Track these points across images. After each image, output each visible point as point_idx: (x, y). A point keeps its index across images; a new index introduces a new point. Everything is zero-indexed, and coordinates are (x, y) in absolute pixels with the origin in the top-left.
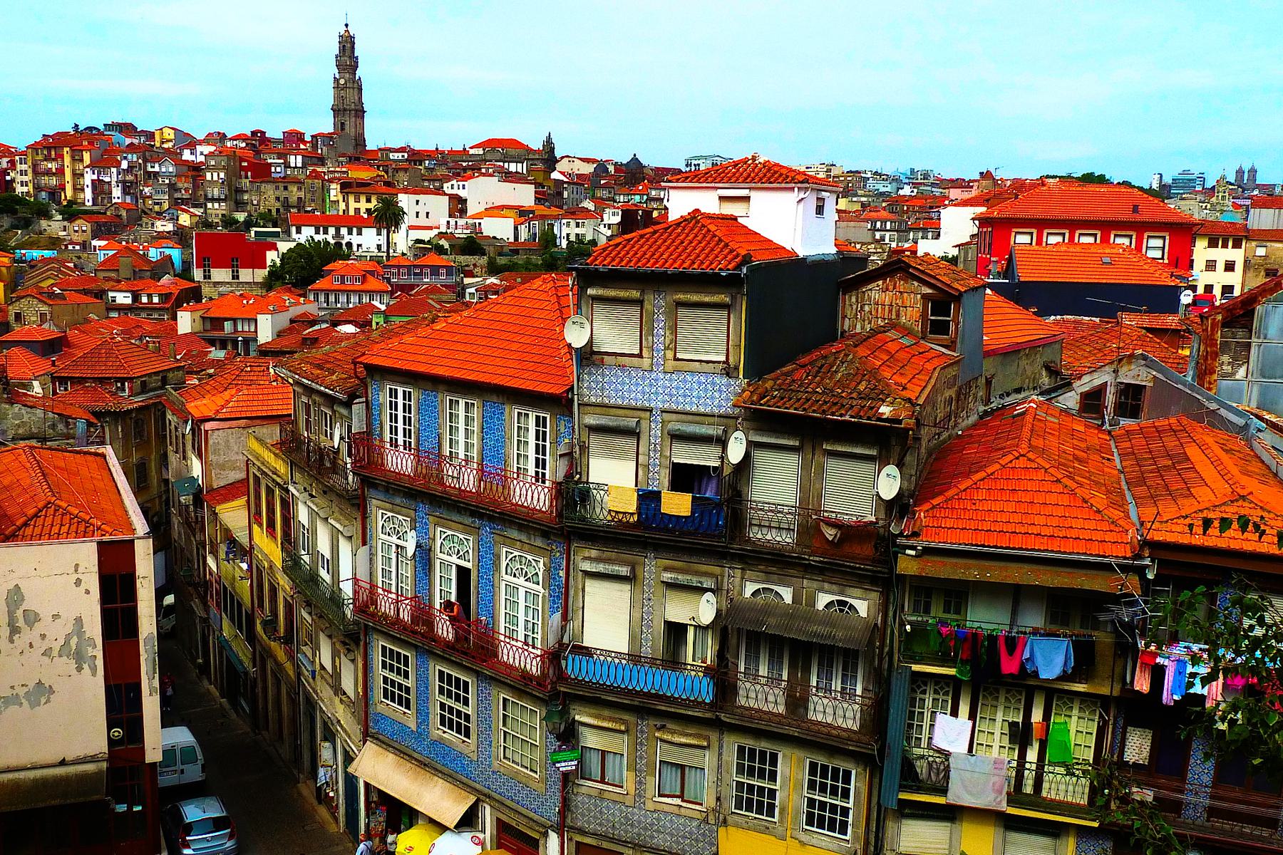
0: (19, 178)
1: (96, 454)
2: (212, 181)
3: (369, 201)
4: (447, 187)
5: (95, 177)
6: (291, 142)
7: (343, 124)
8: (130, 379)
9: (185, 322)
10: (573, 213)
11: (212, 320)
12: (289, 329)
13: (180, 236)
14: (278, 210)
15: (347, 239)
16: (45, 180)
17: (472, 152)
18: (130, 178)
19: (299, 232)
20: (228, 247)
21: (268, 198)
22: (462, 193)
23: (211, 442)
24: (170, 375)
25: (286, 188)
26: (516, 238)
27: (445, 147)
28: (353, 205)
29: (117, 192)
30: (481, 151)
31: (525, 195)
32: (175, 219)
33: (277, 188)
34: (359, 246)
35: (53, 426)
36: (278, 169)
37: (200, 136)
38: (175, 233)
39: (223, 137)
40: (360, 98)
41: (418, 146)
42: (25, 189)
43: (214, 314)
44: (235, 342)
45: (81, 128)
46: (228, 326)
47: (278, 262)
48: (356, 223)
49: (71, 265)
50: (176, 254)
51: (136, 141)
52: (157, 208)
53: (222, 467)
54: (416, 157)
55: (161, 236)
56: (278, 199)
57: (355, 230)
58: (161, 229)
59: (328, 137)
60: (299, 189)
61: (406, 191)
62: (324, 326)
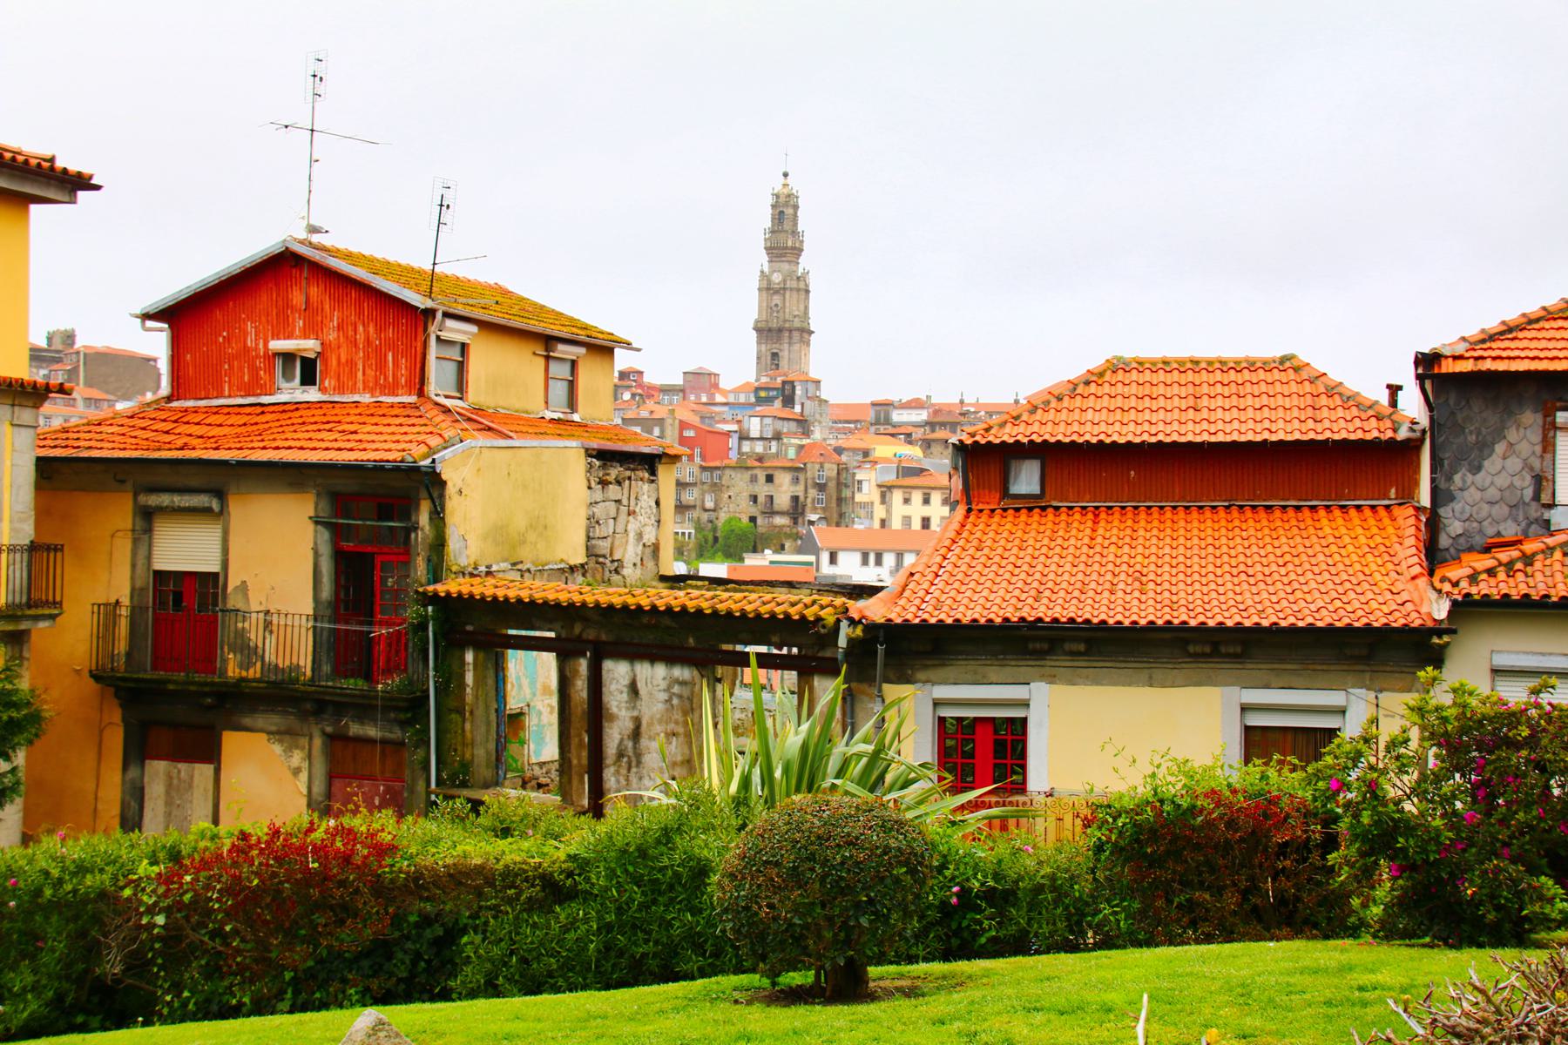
3: (926, 501)
6: (697, 389)
7: (775, 355)
25: (770, 479)
33: (754, 479)
40: (806, 308)
56: (755, 499)
60: (796, 481)
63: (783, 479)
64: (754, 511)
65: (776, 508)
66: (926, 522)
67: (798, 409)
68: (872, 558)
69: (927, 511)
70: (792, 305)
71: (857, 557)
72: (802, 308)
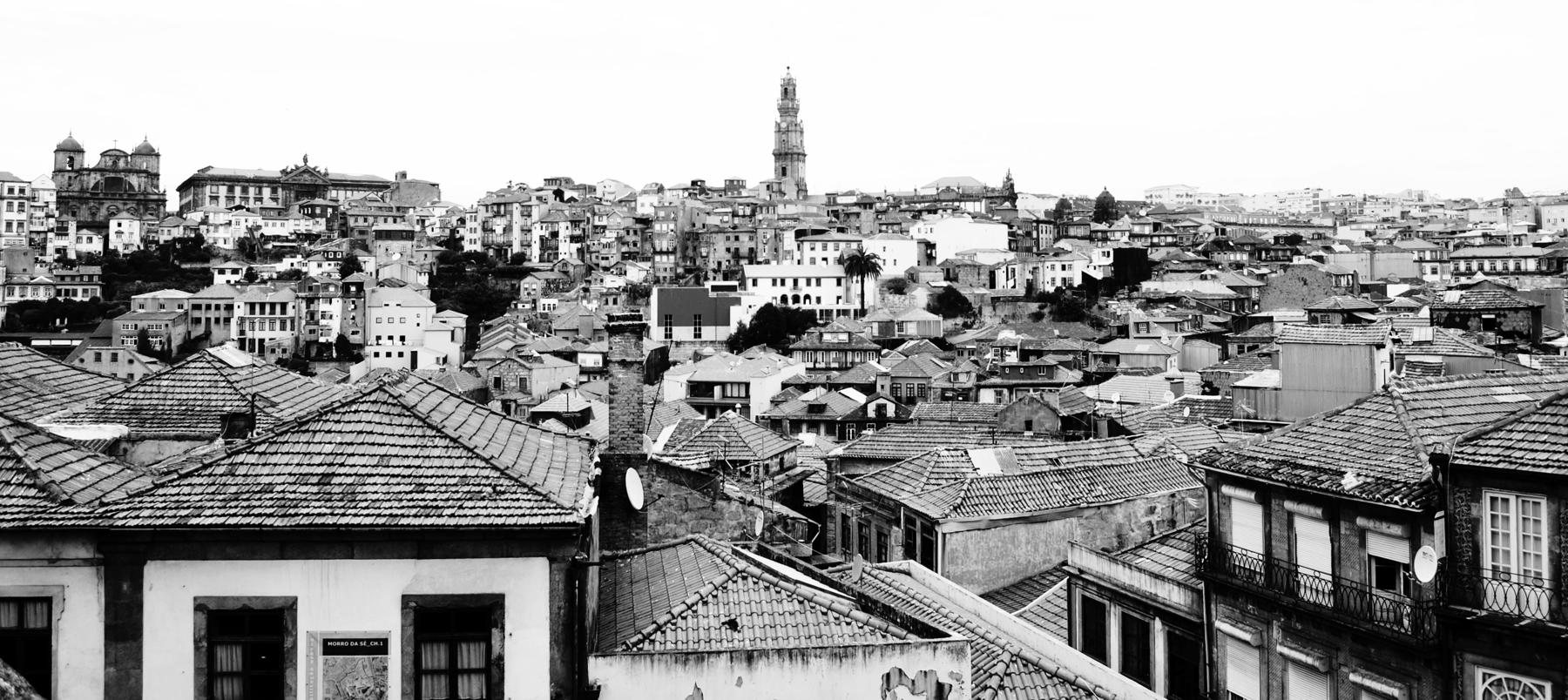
0: (468, 236)
2: (661, 235)
3: (825, 248)
4: (913, 230)
7: (784, 170)
10: (1056, 255)
13: (637, 294)
18: (578, 232)
19: (755, 283)
20: (694, 304)
22: (931, 239)
23: (948, 548)
24: (786, 456)
25: (737, 238)
30: (934, 192)
33: (728, 239)
36: (726, 218)
37: (638, 189)
39: (661, 189)
41: (867, 191)
46: (717, 389)
47: (747, 322)
51: (575, 194)
52: (603, 263)
54: (866, 203)
56: (728, 250)
57: (813, 282)
60: (751, 239)
62: (823, 391)
63: (744, 238)
70: (793, 138)
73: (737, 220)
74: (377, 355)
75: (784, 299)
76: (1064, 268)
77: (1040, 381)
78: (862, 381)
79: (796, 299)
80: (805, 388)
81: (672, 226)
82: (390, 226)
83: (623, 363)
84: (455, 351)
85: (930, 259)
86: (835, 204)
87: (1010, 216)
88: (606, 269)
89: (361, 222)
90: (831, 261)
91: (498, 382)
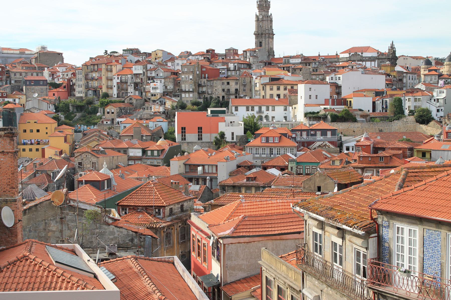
1: (168, 262)
3: (278, 89)
5: (119, 81)
8: (164, 207)
9: (176, 166)
10: (412, 92)
11: (190, 165)
12: (237, 171)
13: (169, 115)
14: (223, 97)
15: (266, 113)
16: (91, 83)
17: (341, 56)
18: (138, 80)
19: (236, 110)
21: (217, 90)
22: (340, 83)
23: (227, 252)
24: (185, 204)
25: (228, 83)
26: (374, 110)
27: (324, 53)
28: (269, 92)
29: (131, 89)
30: (347, 55)
31: (379, 82)
32: (163, 104)
33: (223, 84)
34: (273, 117)
35: (132, 240)
36: (223, 72)
37: (176, 54)
38: (164, 113)
39: (189, 54)
40: (271, 27)
41: (306, 55)
42: (81, 89)
43: (189, 163)
44: (205, 180)
45: (109, 52)
46: (200, 169)
48: (271, 103)
49: (106, 133)
50: (164, 125)
51: (140, 59)
52: (153, 98)
53: (233, 268)
54: (307, 61)
55: (156, 114)
56: (223, 90)
58: (157, 110)
59: (254, 51)
60: (237, 83)
61: (302, 82)
63: (232, 83)
64: (223, 94)
65: (231, 93)
66: (279, 96)
67: (248, 60)
68: (250, 108)
69: (278, 92)
70: (265, 25)
71: (245, 108)
72: (270, 27)
73: (229, 73)
74: (24, 150)
75: (253, 117)
76: (415, 100)
77: (380, 165)
78: (281, 164)
79: (261, 118)
80: (250, 168)
81: (191, 77)
82: (35, 77)
83: (3, 152)
84: (66, 147)
85: (339, 94)
86: (288, 62)
87: (388, 70)
88: (154, 101)
89: (18, 75)
90: (282, 97)
91: (80, 164)
